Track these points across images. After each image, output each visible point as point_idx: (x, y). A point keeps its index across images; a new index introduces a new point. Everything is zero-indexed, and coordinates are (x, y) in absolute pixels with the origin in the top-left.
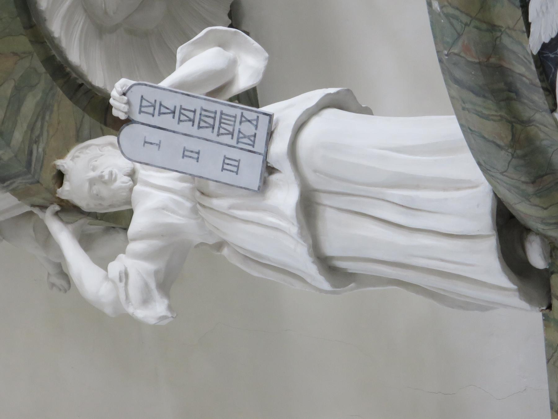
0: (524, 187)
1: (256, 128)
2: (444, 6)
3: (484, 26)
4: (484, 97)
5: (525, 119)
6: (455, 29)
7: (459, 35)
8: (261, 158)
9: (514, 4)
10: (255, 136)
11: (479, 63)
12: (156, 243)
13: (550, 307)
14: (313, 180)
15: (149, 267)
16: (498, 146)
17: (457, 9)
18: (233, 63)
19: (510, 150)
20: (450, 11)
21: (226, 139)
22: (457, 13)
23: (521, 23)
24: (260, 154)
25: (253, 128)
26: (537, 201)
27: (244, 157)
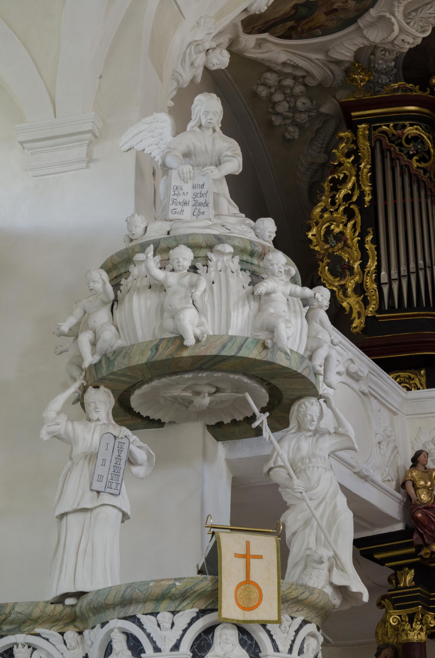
0: (92, 605)
1: (115, 489)
2: (151, 588)
3: (145, 600)
4: (121, 598)
5: (115, 608)
6: (143, 591)
7: (141, 592)
8: (103, 491)
9: (153, 610)
10: (111, 488)
11: (132, 598)
12: (71, 435)
13: (52, 603)
14: (95, 512)
15: (62, 432)
16: (105, 600)
17: (150, 592)
18: (141, 465)
19: (104, 603)
20: (150, 590)
21: (110, 477)
22: (149, 592)
23: (147, 612)
24: (105, 490)
25: (114, 488)
26: (88, 607)
27: (104, 484)
